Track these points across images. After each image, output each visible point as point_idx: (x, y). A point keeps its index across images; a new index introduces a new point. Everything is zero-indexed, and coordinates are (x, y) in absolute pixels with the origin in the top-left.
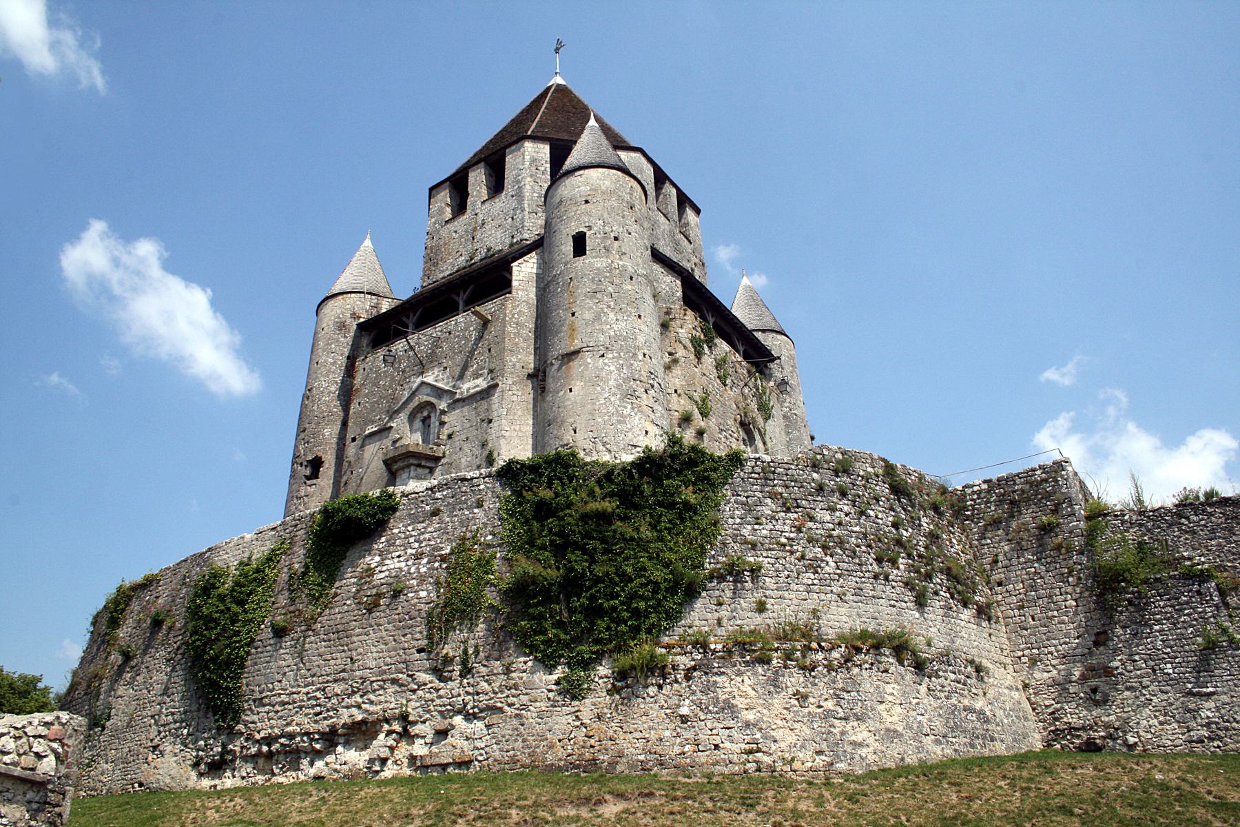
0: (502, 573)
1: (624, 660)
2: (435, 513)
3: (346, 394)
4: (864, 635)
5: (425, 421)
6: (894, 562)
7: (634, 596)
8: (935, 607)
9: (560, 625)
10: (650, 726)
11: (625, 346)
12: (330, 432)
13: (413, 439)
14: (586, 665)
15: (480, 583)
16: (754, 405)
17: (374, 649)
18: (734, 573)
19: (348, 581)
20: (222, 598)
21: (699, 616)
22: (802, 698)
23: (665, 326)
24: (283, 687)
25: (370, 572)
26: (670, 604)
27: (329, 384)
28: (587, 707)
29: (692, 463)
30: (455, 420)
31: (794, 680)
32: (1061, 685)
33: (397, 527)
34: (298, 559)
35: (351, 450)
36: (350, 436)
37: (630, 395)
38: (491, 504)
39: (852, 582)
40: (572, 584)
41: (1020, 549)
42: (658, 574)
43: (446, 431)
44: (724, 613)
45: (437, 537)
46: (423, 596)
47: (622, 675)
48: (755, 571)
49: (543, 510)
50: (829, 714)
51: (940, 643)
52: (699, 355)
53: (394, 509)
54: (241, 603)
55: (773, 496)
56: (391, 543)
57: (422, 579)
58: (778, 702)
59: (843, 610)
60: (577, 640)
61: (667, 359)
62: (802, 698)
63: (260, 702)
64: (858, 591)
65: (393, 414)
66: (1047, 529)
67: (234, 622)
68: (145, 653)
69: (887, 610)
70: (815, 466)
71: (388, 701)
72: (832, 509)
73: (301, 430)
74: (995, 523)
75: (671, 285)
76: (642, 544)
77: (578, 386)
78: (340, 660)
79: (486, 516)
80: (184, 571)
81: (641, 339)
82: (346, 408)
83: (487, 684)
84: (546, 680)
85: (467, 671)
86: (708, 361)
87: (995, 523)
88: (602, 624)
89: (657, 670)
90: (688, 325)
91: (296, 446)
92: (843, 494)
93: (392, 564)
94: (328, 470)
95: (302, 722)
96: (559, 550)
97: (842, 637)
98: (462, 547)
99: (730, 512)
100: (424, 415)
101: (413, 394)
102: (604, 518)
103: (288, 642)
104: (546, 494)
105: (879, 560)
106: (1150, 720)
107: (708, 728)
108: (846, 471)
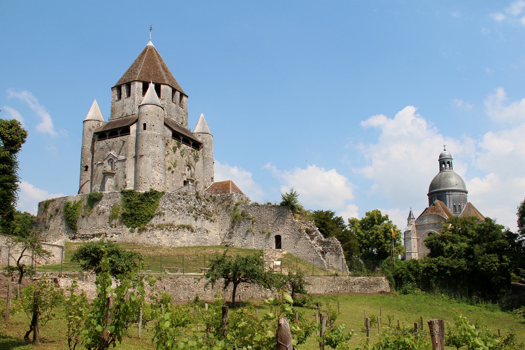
0: (121, 211)
1: (140, 228)
2: (110, 198)
3: (93, 151)
4: (182, 226)
5: (112, 162)
6: (192, 212)
7: (142, 217)
8: (199, 221)
9: (130, 221)
10: (143, 238)
11: (154, 154)
12: (89, 159)
13: (109, 168)
14: (134, 228)
15: (118, 212)
16: (192, 159)
17: (101, 221)
18: (160, 214)
19: (95, 209)
20: (71, 208)
21: (153, 221)
22: (168, 235)
23: (167, 144)
24: (84, 227)
25: (99, 208)
26: (148, 219)
27: (88, 146)
28: (134, 234)
29: (155, 194)
30: (118, 165)
31: (167, 232)
32: (225, 234)
33: (103, 200)
34: (85, 203)
35: (95, 166)
36: (94, 163)
37: (154, 166)
38: (120, 198)
39: (182, 216)
40: (132, 215)
41: (223, 209)
42: (146, 214)
43: (116, 167)
44: (157, 221)
45: (110, 202)
46: (108, 213)
47: (139, 230)
48: (164, 214)
49: (128, 201)
50: (173, 238)
51: (199, 227)
52: (174, 152)
53: (103, 196)
54: (75, 210)
55: (170, 200)
56: (102, 203)
57: (108, 210)
58: (164, 236)
59: (179, 221)
60: (133, 224)
61: (167, 153)
62: (168, 235)
63: (81, 228)
64: (183, 218)
65: (104, 160)
66: (228, 206)
67: (74, 213)
68: (56, 215)
69: (189, 221)
70: (179, 194)
71: (103, 231)
72: (181, 202)
73: (82, 158)
74: (220, 203)
75: (170, 133)
76: (144, 208)
77: (143, 164)
78: (95, 223)
79: (119, 199)
80: (61, 200)
81: (158, 152)
82: (93, 154)
83: (119, 229)
84: (128, 229)
85: (116, 227)
86: (178, 151)
87: (220, 203)
88: (137, 221)
89: (144, 229)
90: (173, 143)
91: (81, 162)
92: (184, 199)
93: (103, 207)
94: (90, 169)
95: (88, 233)
96: (131, 208)
97: (178, 226)
98: (115, 205)
99: (161, 203)
100: (111, 161)
101: (108, 156)
102: (138, 204)
103: (85, 219)
104: (129, 198)
105: (188, 212)
106: (237, 242)
107: (152, 239)
108: (186, 195)
